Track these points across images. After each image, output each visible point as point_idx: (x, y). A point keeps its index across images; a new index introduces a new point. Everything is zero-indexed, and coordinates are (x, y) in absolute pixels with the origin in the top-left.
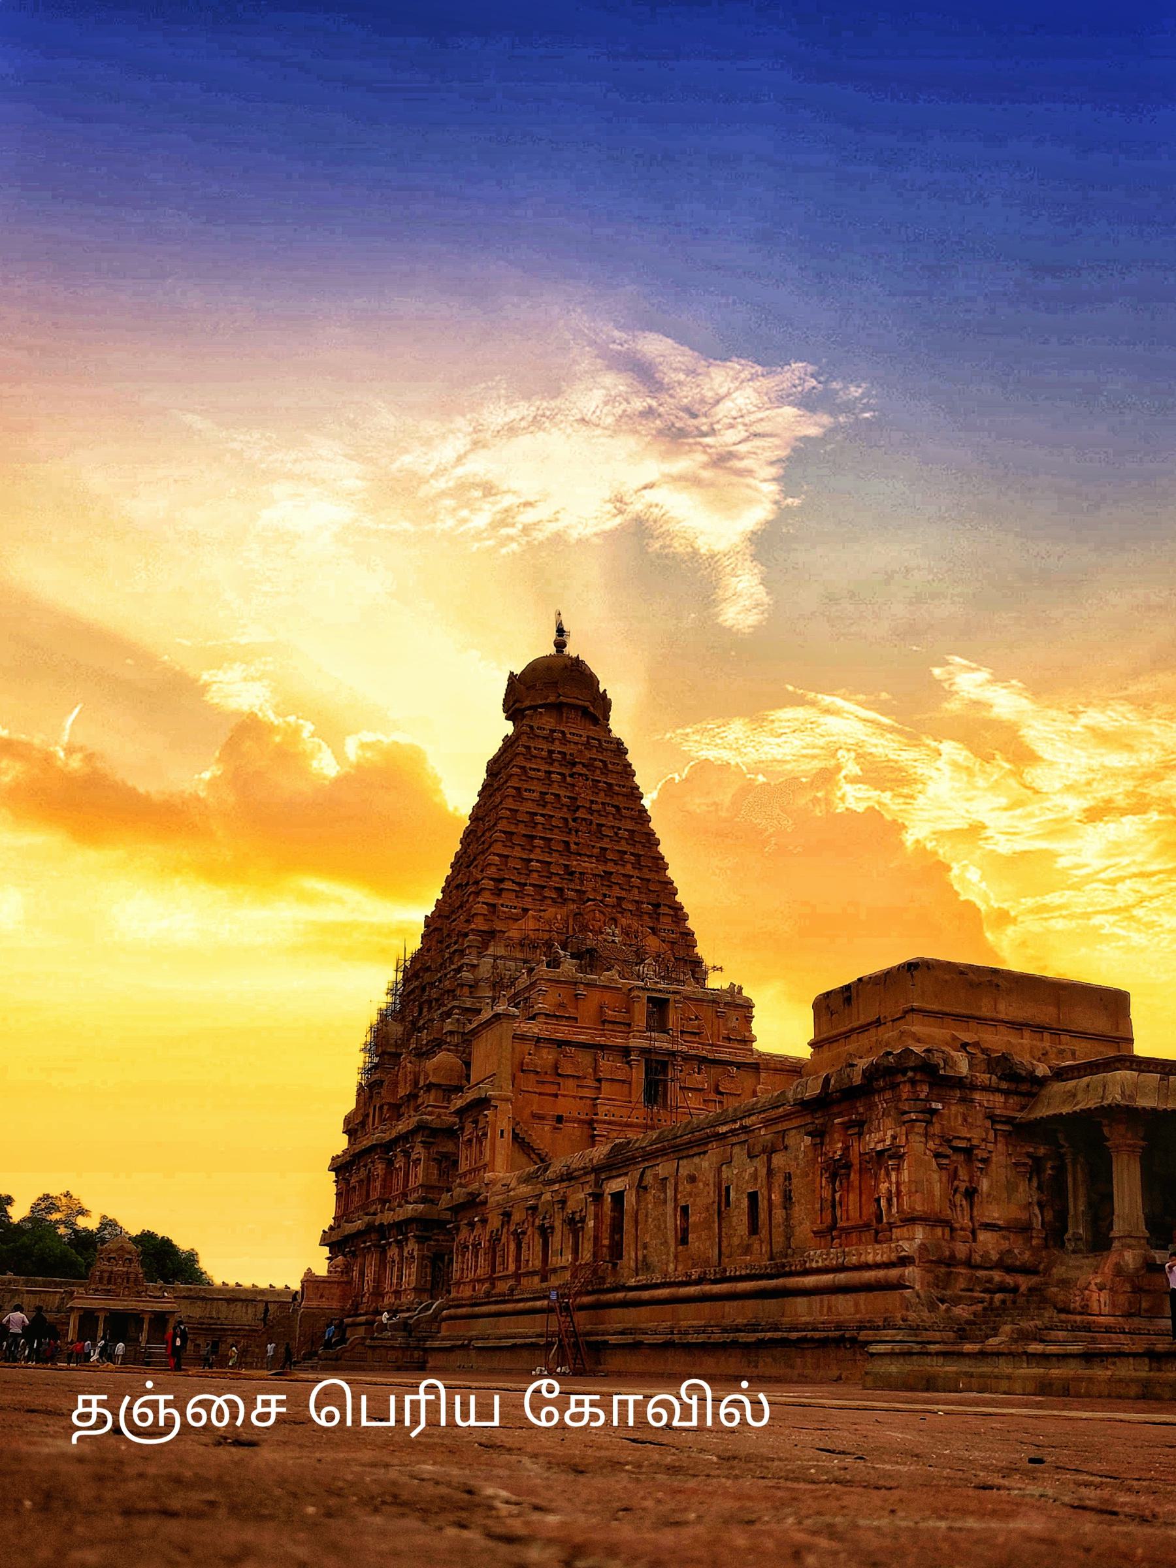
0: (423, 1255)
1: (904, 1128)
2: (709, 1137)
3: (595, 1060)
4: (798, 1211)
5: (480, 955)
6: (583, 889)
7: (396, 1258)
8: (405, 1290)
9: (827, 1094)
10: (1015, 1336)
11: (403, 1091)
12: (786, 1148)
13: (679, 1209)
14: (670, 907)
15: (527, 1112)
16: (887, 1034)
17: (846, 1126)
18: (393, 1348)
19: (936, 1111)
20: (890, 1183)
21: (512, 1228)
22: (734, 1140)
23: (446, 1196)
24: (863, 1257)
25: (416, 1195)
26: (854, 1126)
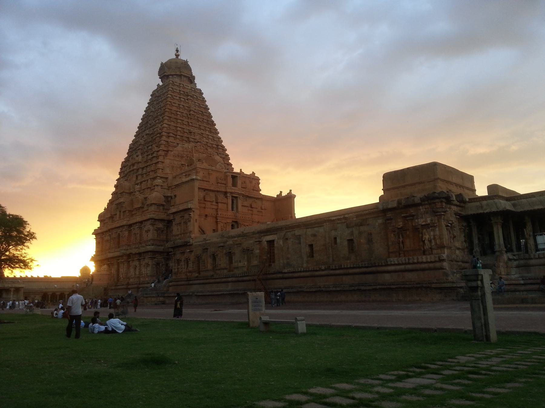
1: (436, 218)
2: (325, 221)
3: (215, 196)
6: (195, 138)
13: (307, 246)
14: (221, 146)
18: (154, 297)
22: (339, 222)
25: (149, 243)
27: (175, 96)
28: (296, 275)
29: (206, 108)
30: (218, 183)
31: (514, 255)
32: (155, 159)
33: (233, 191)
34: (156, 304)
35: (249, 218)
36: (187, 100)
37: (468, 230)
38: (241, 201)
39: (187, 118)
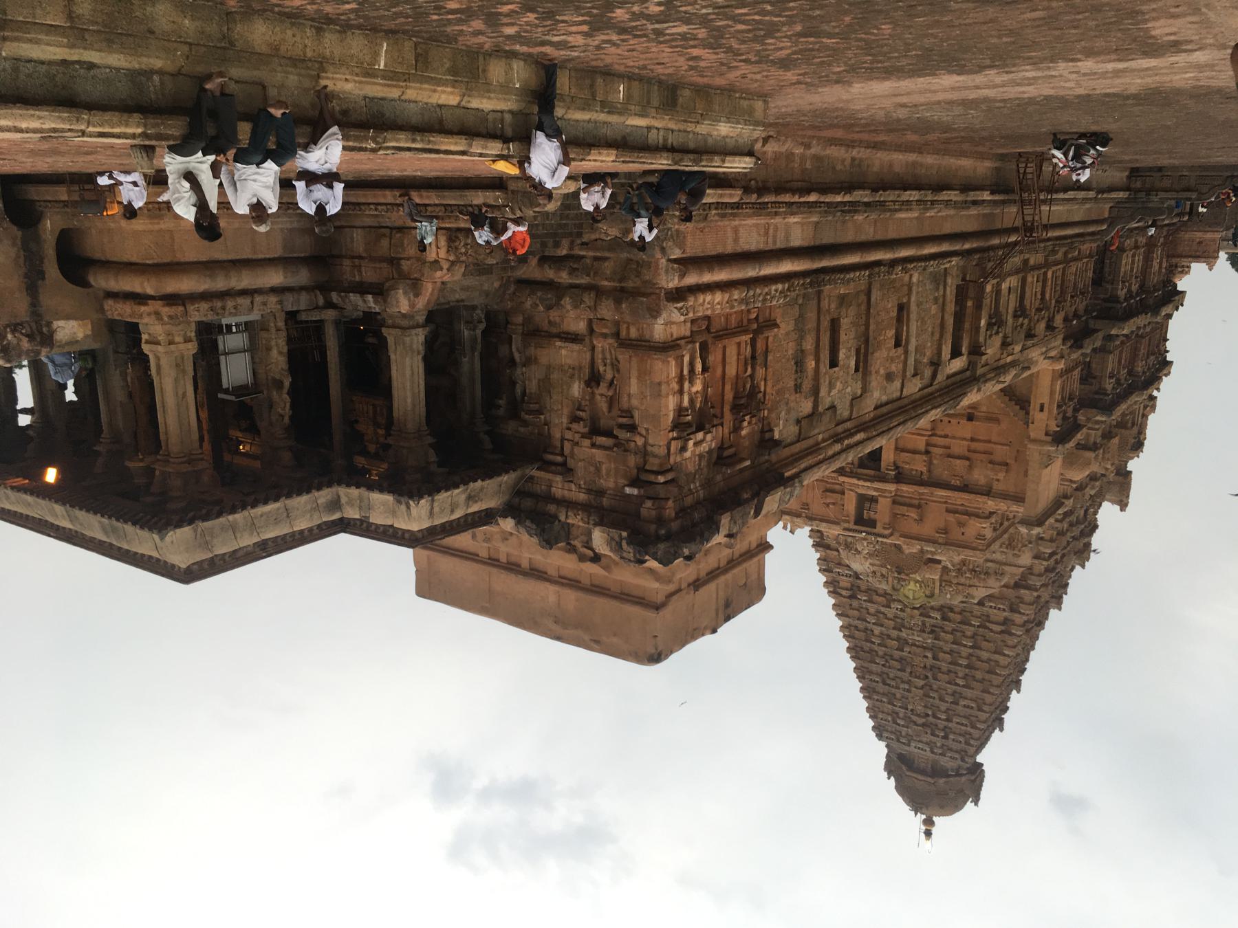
0: (1112, 284)
2: (873, 425)
4: (791, 349)
5: (1030, 568)
6: (922, 618)
7: (1134, 281)
11: (1116, 441)
12: (798, 422)
14: (841, 595)
17: (735, 459)
18: (1166, 190)
19: (632, 484)
22: (848, 425)
23: (1098, 344)
24: (726, 299)
26: (730, 457)
27: (962, 724)
28: (945, 247)
34: (1160, 169)
36: (927, 715)
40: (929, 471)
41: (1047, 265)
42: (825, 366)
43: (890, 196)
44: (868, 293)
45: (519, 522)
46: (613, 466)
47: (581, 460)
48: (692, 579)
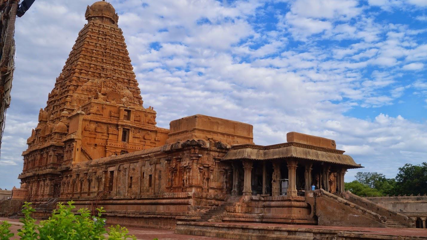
4: (163, 181)
6: (107, 74)
7: (43, 185)
8: (45, 195)
9: (172, 150)
10: (215, 219)
11: (47, 133)
12: (160, 163)
13: (129, 178)
14: (133, 81)
15: (86, 142)
16: (189, 135)
17: (177, 159)
18: (41, 213)
20: (187, 176)
21: (80, 179)
22: (146, 159)
23: (59, 168)
25: (50, 166)
27: (94, 36)
28: (119, 202)
29: (124, 46)
30: (111, 116)
31: (263, 197)
32: (66, 92)
33: (124, 124)
35: (140, 148)
36: (105, 39)
37: (230, 173)
38: (132, 133)
39: (102, 55)
40: (108, 128)
41: (81, 193)
42: (153, 176)
43: (138, 216)
44: (140, 192)
45: (226, 147)
46: (204, 160)
47: (211, 161)
48: (187, 133)
